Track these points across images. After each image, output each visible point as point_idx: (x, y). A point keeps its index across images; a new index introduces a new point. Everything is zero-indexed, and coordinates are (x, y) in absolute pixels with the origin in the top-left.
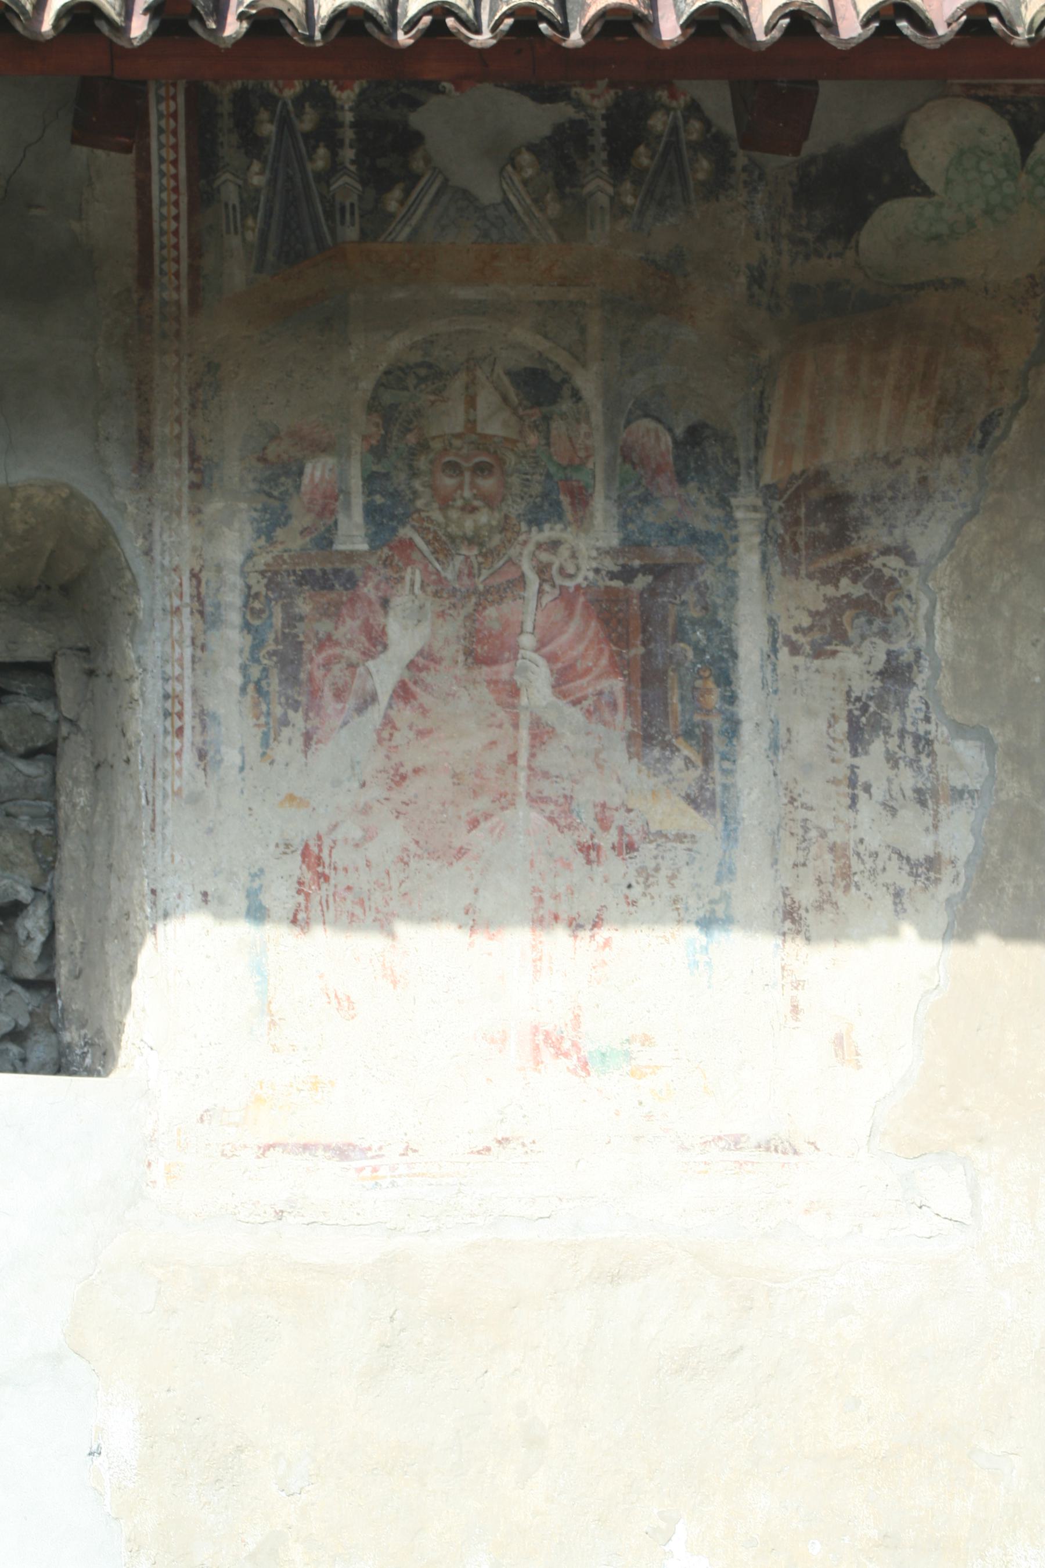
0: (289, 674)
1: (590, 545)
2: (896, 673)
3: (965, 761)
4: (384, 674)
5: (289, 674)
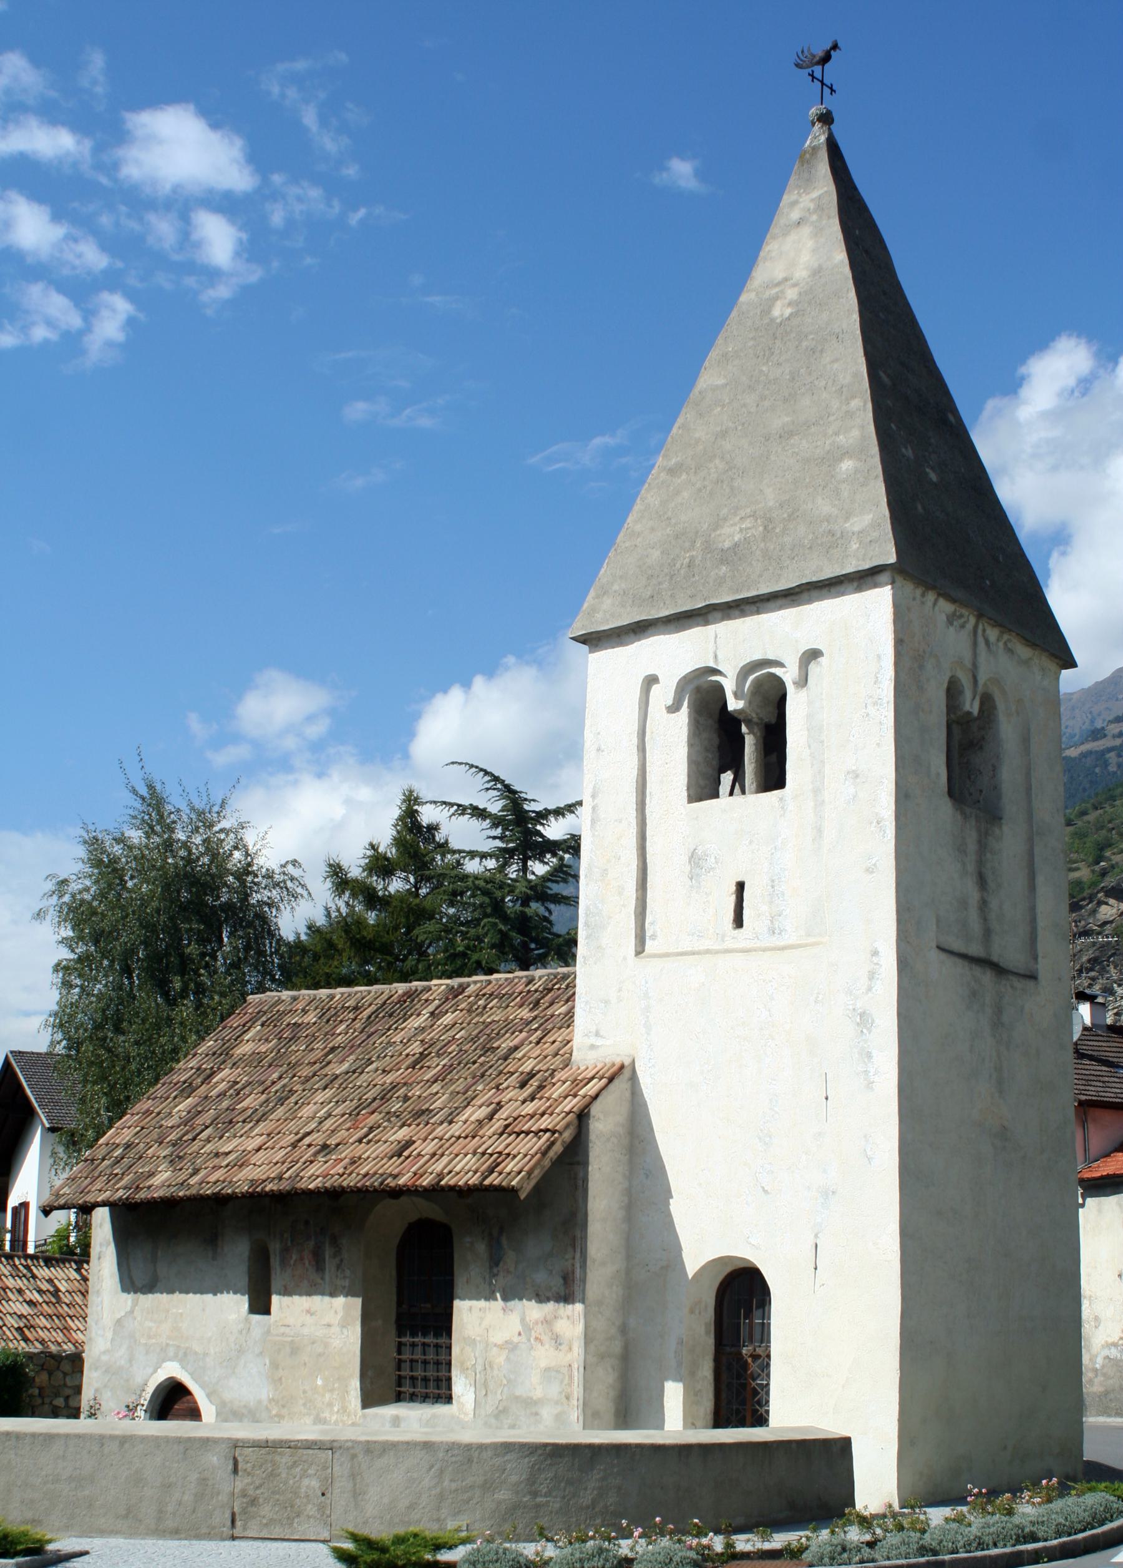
0: (284, 1263)
1: (311, 1244)
2: (342, 1260)
3: (348, 1273)
4: (292, 1262)
5: (284, 1263)
